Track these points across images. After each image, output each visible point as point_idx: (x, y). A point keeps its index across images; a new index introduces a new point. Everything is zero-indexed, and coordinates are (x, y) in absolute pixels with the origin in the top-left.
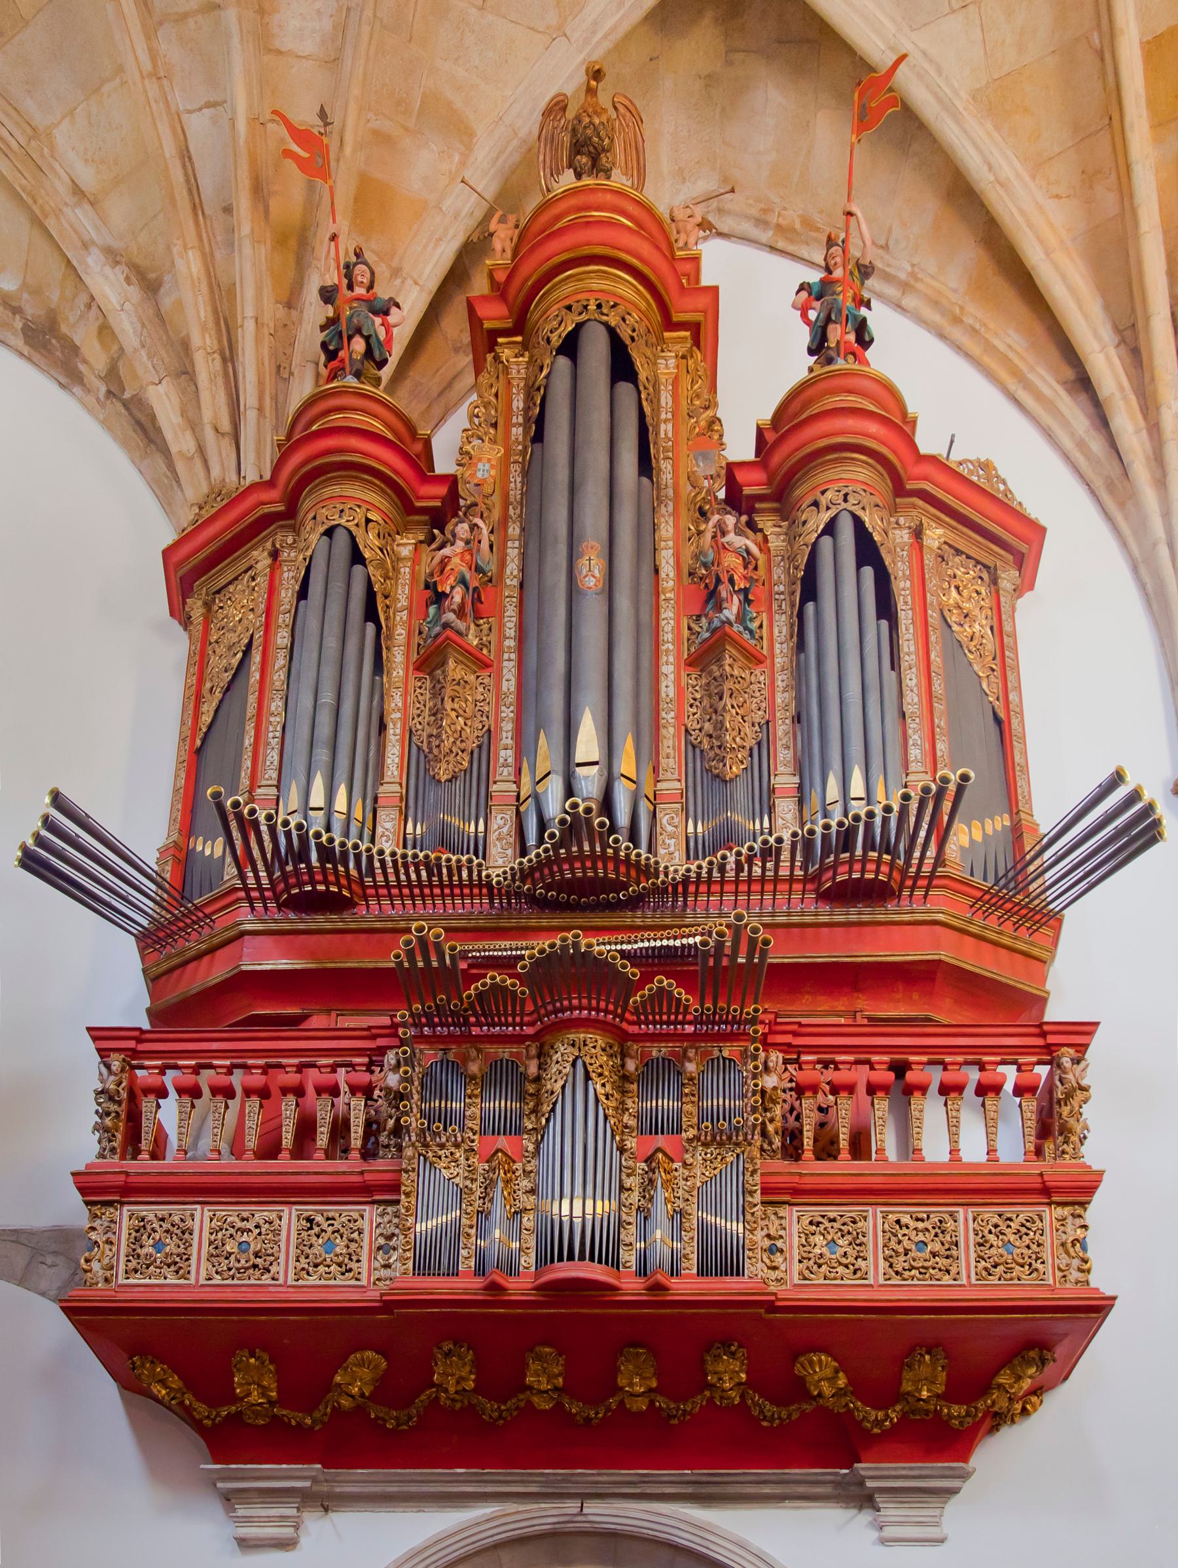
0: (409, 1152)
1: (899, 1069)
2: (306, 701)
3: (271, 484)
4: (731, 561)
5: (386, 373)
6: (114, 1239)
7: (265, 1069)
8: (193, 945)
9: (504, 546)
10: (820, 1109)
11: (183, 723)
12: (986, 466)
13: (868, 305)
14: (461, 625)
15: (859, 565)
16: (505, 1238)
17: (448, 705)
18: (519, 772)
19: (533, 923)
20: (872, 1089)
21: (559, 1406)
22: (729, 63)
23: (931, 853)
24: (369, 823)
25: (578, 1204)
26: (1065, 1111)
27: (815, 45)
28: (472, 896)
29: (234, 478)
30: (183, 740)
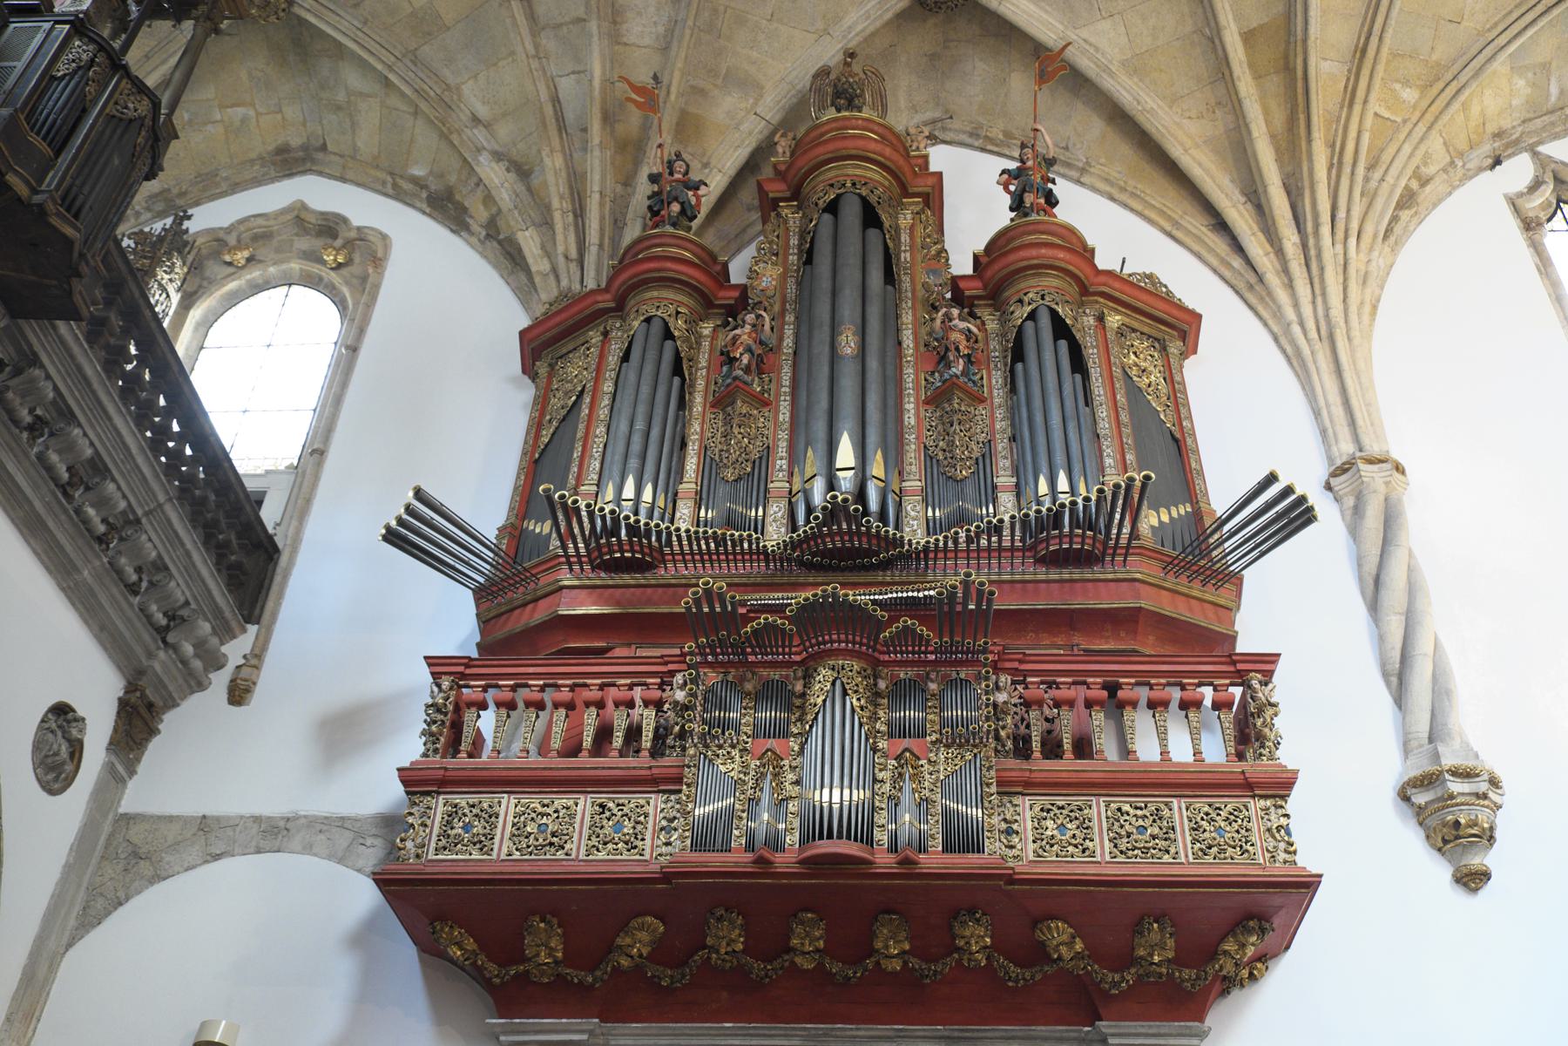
0: (692, 751)
1: (1112, 688)
2: (624, 427)
3: (607, 290)
4: (955, 336)
5: (695, 224)
6: (429, 822)
7: (572, 688)
8: (518, 595)
9: (782, 328)
10: (1047, 720)
11: (526, 442)
12: (1150, 276)
13: (1053, 182)
14: (748, 378)
15: (1056, 339)
16: (772, 821)
17: (736, 430)
18: (791, 474)
19: (801, 580)
20: (1089, 704)
21: (820, 965)
22: (946, 47)
23: (1126, 530)
24: (670, 510)
25: (836, 792)
26: (1259, 722)
27: (1006, 35)
28: (751, 561)
29: (578, 286)
30: (524, 454)
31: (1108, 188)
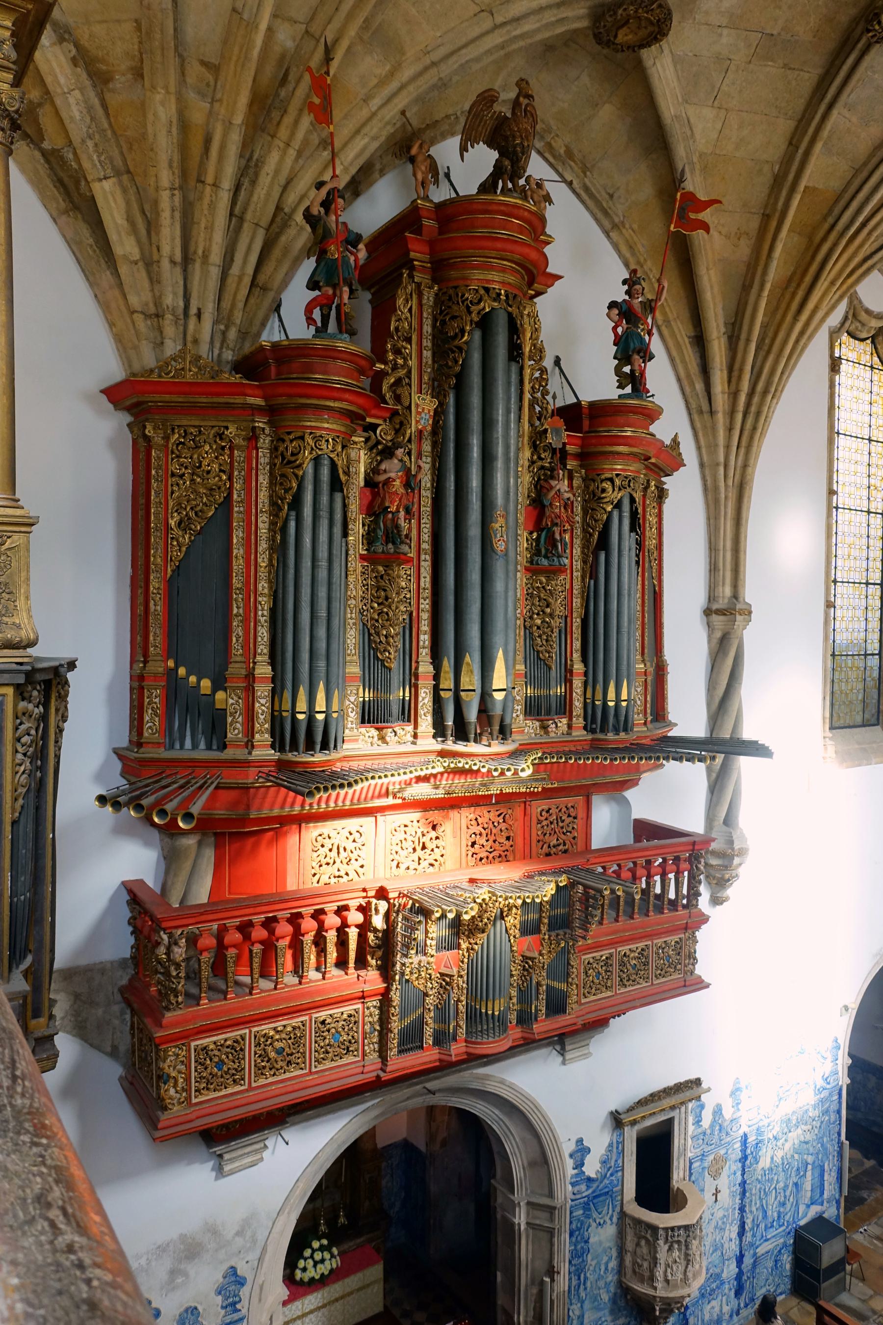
22: (566, 44)
31: (628, 255)
